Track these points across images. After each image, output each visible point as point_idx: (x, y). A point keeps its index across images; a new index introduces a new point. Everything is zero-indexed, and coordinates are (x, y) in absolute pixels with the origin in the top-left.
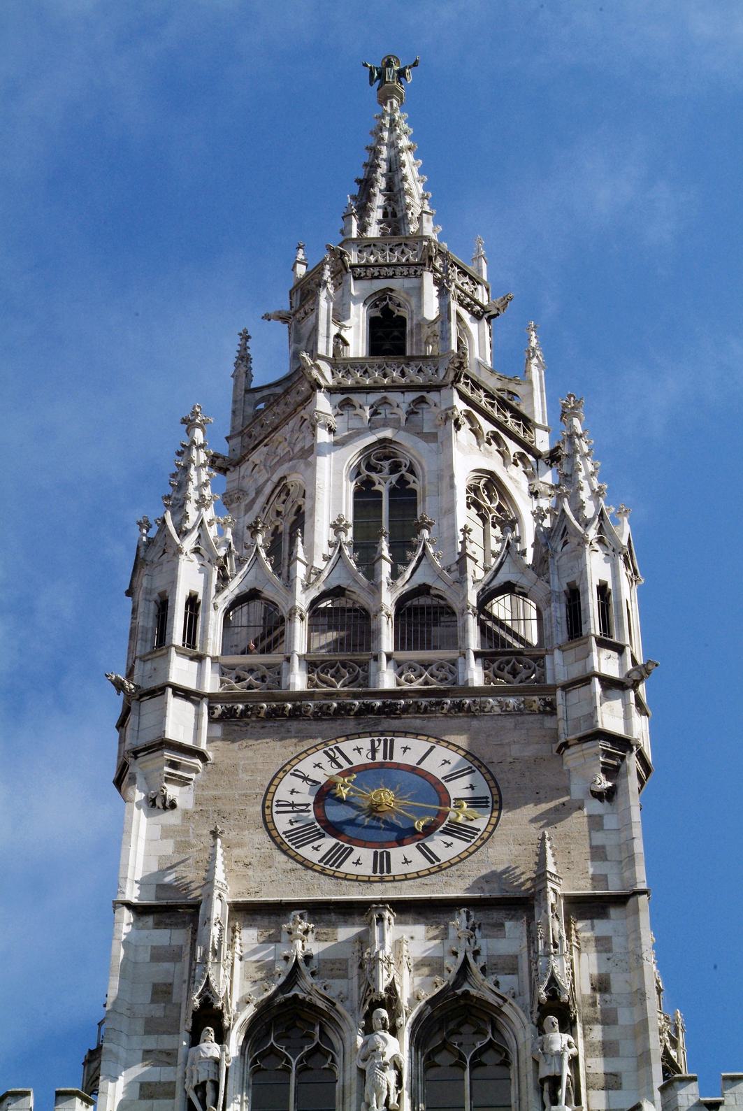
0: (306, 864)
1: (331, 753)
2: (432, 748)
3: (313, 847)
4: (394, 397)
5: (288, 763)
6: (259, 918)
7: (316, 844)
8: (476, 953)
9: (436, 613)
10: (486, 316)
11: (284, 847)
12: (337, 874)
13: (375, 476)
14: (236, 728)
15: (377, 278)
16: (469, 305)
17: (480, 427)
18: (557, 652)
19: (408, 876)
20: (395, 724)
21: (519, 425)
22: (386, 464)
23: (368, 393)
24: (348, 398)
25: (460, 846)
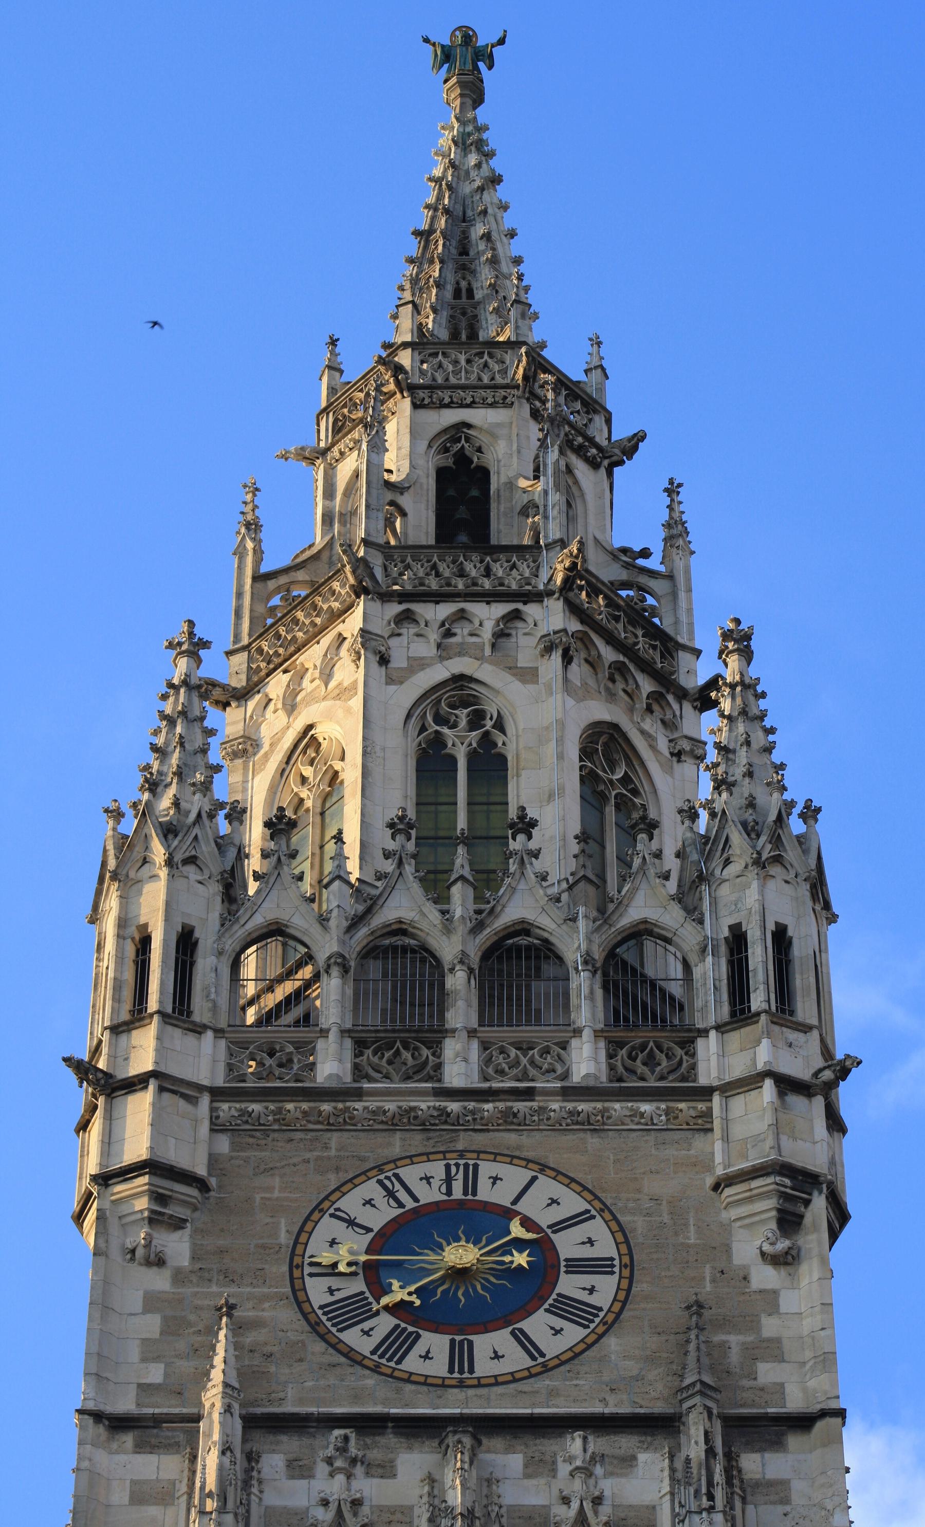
0: (351, 1356)
1: (387, 1182)
2: (534, 1179)
3: (362, 1330)
4: (478, 610)
5: (326, 1198)
6: (284, 1438)
7: (366, 1325)
8: (597, 1501)
9: (538, 958)
10: (606, 463)
11: (321, 1330)
12: (396, 1374)
13: (445, 730)
14: (251, 1140)
15: (447, 406)
16: (581, 446)
17: (599, 656)
18: (713, 1034)
19: (500, 1379)
20: (480, 1140)
21: (654, 647)
22: (463, 714)
23: (437, 603)
24: (408, 610)
25: (574, 1334)
